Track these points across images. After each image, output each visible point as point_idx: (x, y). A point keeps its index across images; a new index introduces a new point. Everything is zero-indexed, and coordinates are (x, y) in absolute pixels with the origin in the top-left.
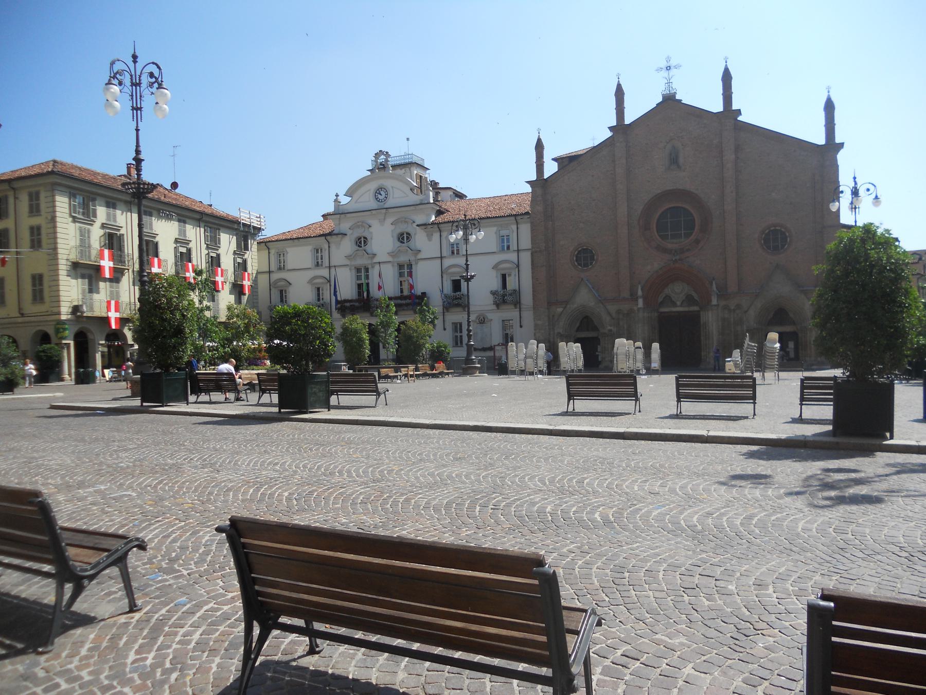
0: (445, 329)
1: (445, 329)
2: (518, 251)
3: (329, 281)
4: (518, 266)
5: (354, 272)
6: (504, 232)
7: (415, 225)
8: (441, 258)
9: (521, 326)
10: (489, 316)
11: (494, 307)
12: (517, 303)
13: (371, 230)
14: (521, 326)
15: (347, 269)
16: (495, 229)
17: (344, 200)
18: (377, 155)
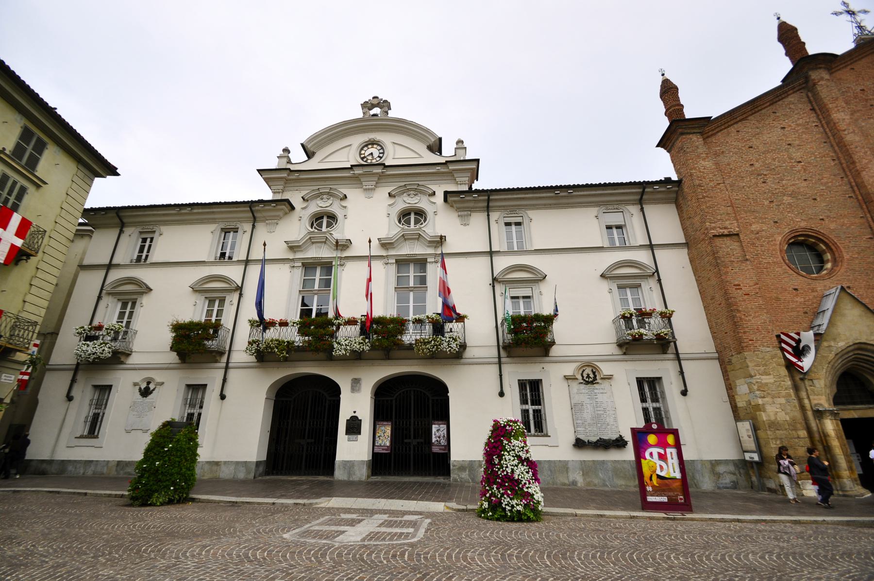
0: (502, 394)
1: (502, 394)
2: (651, 247)
3: (240, 289)
4: (657, 271)
5: (299, 273)
6: (615, 219)
7: (439, 198)
8: (491, 253)
9: (684, 393)
10: (606, 369)
11: (613, 349)
12: (663, 344)
13: (344, 203)
14: (684, 393)
15: (286, 267)
16: (593, 211)
17: (298, 156)
18: (367, 106)
